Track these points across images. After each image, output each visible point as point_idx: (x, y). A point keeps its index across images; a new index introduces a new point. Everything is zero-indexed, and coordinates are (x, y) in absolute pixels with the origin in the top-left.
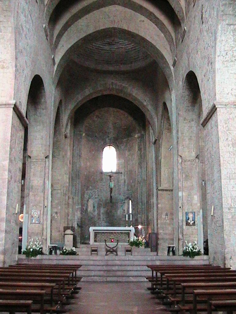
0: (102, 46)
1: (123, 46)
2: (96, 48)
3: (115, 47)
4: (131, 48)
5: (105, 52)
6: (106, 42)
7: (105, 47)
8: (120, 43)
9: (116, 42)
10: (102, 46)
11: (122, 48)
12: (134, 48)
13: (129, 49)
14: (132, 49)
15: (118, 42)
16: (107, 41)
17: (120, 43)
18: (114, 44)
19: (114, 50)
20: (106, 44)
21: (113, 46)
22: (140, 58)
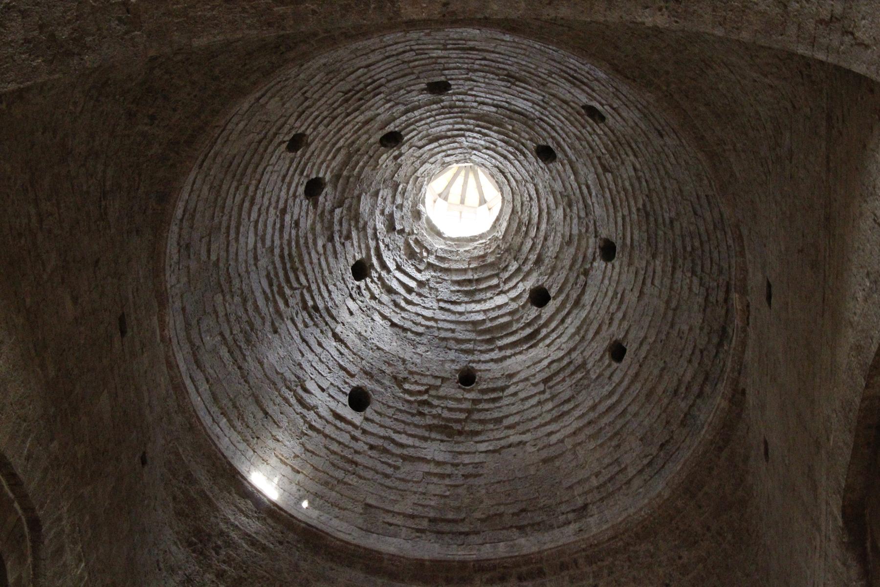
0: (403, 439)
1: (524, 438)
2: (372, 447)
3: (483, 447)
4: (574, 433)
5: (429, 474)
6: (429, 421)
7: (424, 445)
8: (506, 422)
9: (482, 422)
10: (410, 441)
11: (521, 443)
12: (589, 431)
13: (562, 441)
14: (581, 437)
15: (498, 421)
16: (434, 416)
17: (506, 422)
18: (477, 433)
19: (477, 459)
20: (430, 428)
21: (469, 445)
22: (631, 471)
